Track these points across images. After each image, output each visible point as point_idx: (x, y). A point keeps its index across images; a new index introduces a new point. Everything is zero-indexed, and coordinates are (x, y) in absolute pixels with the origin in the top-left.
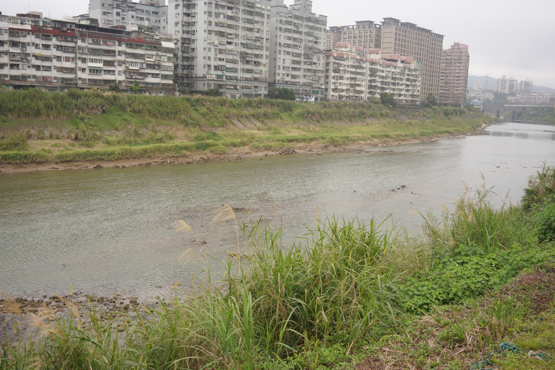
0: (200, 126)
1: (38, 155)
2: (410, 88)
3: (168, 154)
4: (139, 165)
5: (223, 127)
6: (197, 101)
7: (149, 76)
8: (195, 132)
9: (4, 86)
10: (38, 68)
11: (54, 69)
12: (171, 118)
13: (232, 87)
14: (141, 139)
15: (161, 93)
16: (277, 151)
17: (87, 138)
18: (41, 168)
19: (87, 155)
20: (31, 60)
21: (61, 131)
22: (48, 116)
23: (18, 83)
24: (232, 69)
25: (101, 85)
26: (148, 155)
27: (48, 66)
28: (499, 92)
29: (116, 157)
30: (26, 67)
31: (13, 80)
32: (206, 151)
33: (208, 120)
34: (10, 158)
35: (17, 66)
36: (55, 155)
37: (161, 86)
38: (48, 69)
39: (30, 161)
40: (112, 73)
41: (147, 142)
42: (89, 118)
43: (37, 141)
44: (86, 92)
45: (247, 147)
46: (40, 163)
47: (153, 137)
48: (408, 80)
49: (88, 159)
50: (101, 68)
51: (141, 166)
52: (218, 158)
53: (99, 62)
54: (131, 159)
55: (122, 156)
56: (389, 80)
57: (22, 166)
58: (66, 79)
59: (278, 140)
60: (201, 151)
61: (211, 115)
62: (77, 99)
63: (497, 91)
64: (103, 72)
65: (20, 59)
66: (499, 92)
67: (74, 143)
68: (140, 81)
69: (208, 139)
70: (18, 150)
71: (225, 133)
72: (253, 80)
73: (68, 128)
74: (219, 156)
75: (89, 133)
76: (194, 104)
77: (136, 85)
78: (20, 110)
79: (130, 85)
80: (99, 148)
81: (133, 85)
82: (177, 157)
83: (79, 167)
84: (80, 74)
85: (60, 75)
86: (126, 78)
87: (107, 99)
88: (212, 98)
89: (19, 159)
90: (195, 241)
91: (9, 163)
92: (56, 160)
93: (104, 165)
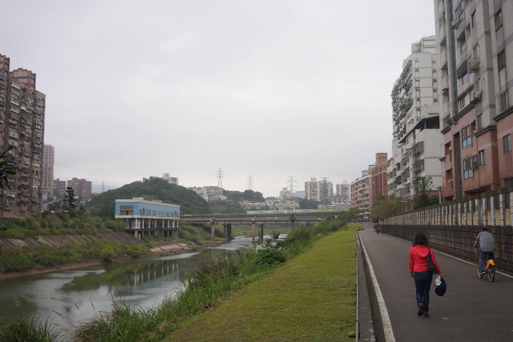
28: (309, 199)
63: (306, 199)
66: (309, 199)
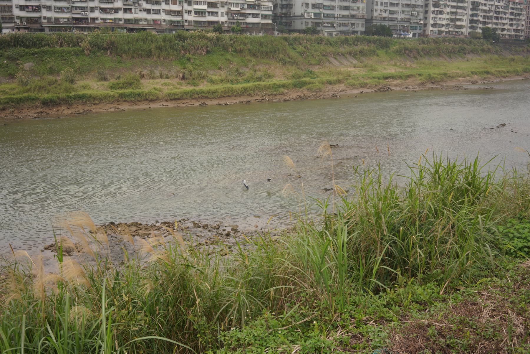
0: (297, 64)
1: (150, 94)
2: (514, 22)
3: (267, 92)
4: (240, 103)
5: (319, 65)
6: (295, 39)
7: (249, 16)
8: (293, 70)
9: (119, 30)
10: (148, 11)
11: (163, 12)
12: (270, 57)
13: (329, 25)
14: (241, 78)
15: (260, 33)
16: (372, 88)
17: (193, 77)
18: (154, 106)
19: (193, 93)
20: (142, 4)
21: (170, 71)
22: (159, 57)
23: (131, 26)
24: (329, 6)
25: (205, 26)
26: (248, 93)
27: (157, 10)
29: (219, 95)
30: (138, 11)
31: (127, 23)
32: (302, 89)
33: (305, 58)
34: (125, 96)
35: (130, 10)
36: (165, 93)
37: (260, 26)
38: (158, 12)
39: (143, 99)
40: (215, 15)
41: (247, 81)
42: (195, 59)
43: (149, 81)
44: (192, 34)
45: (343, 85)
46: (152, 101)
47: (252, 76)
48: (512, 14)
49: (194, 97)
50: (205, 10)
51: (242, 104)
52: (314, 95)
53: (204, 5)
54: (233, 97)
55: (225, 94)
56: (491, 14)
57: (137, 103)
58: (174, 22)
59: (374, 78)
60: (297, 89)
61: (308, 54)
62: (184, 40)
64: (207, 14)
65: (132, 4)
67: (182, 82)
68: (241, 21)
69: (304, 77)
70: (133, 89)
71: (321, 71)
72: (350, 17)
73: (176, 68)
74: (315, 93)
75: (195, 73)
76: (292, 43)
77: (238, 26)
78: (134, 51)
79: (232, 26)
80: (204, 86)
81: (234, 26)
82: (275, 95)
83: (186, 104)
84: (186, 17)
85: (169, 18)
86: (229, 19)
87: (211, 40)
88: (309, 36)
89: (134, 97)
90: (291, 175)
91: (125, 101)
92: (166, 98)
93: (209, 102)
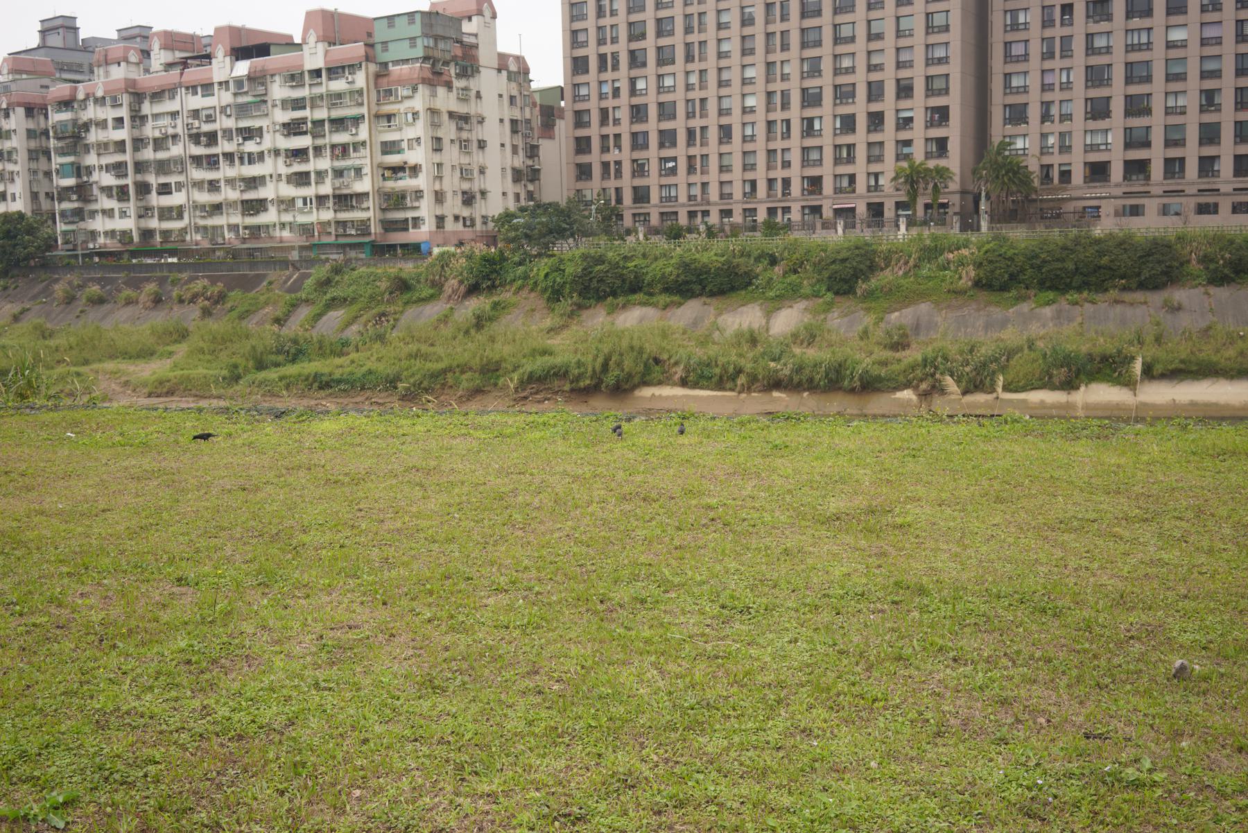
2: (314, 165)
48: (293, 128)
56: (176, 150)
